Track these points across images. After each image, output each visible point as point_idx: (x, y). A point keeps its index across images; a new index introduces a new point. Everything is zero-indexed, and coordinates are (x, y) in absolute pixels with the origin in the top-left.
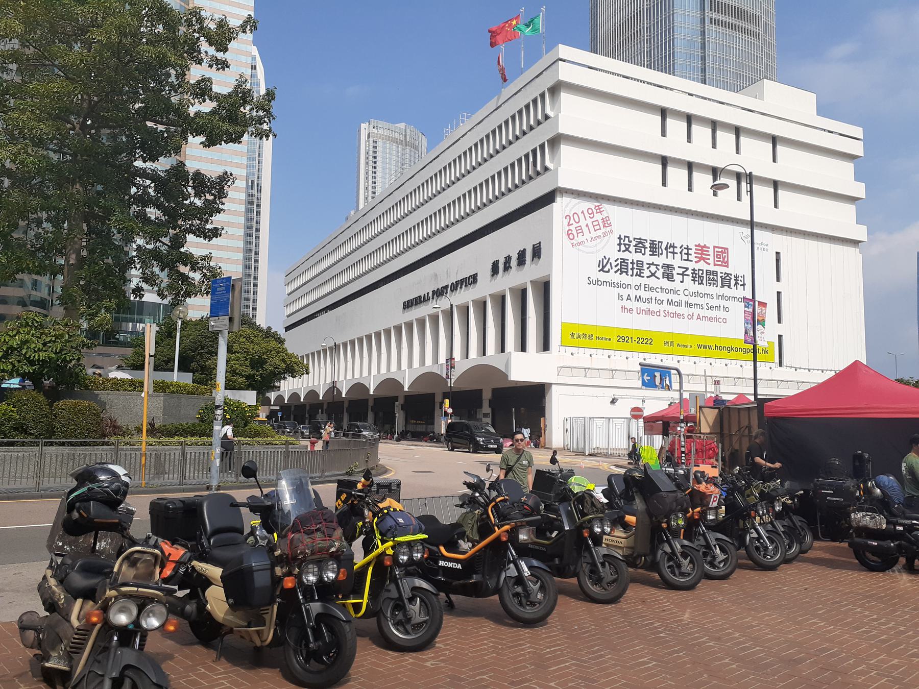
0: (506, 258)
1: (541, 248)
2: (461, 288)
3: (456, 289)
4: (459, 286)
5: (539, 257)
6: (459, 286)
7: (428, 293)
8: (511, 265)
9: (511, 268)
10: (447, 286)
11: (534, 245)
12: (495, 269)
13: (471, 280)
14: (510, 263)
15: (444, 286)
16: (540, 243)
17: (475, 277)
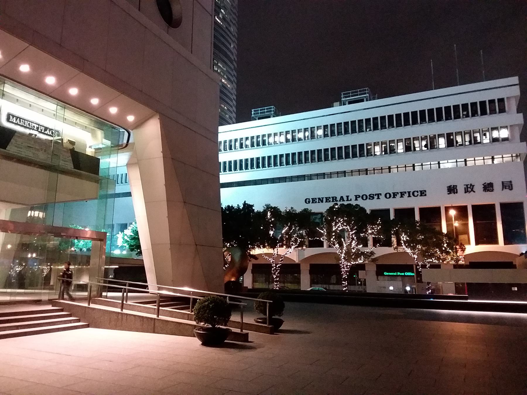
0: (467, 185)
1: (512, 185)
4: (400, 195)
5: (511, 189)
7: (348, 197)
9: (474, 192)
10: (381, 194)
11: (503, 182)
13: (416, 194)
16: (511, 182)
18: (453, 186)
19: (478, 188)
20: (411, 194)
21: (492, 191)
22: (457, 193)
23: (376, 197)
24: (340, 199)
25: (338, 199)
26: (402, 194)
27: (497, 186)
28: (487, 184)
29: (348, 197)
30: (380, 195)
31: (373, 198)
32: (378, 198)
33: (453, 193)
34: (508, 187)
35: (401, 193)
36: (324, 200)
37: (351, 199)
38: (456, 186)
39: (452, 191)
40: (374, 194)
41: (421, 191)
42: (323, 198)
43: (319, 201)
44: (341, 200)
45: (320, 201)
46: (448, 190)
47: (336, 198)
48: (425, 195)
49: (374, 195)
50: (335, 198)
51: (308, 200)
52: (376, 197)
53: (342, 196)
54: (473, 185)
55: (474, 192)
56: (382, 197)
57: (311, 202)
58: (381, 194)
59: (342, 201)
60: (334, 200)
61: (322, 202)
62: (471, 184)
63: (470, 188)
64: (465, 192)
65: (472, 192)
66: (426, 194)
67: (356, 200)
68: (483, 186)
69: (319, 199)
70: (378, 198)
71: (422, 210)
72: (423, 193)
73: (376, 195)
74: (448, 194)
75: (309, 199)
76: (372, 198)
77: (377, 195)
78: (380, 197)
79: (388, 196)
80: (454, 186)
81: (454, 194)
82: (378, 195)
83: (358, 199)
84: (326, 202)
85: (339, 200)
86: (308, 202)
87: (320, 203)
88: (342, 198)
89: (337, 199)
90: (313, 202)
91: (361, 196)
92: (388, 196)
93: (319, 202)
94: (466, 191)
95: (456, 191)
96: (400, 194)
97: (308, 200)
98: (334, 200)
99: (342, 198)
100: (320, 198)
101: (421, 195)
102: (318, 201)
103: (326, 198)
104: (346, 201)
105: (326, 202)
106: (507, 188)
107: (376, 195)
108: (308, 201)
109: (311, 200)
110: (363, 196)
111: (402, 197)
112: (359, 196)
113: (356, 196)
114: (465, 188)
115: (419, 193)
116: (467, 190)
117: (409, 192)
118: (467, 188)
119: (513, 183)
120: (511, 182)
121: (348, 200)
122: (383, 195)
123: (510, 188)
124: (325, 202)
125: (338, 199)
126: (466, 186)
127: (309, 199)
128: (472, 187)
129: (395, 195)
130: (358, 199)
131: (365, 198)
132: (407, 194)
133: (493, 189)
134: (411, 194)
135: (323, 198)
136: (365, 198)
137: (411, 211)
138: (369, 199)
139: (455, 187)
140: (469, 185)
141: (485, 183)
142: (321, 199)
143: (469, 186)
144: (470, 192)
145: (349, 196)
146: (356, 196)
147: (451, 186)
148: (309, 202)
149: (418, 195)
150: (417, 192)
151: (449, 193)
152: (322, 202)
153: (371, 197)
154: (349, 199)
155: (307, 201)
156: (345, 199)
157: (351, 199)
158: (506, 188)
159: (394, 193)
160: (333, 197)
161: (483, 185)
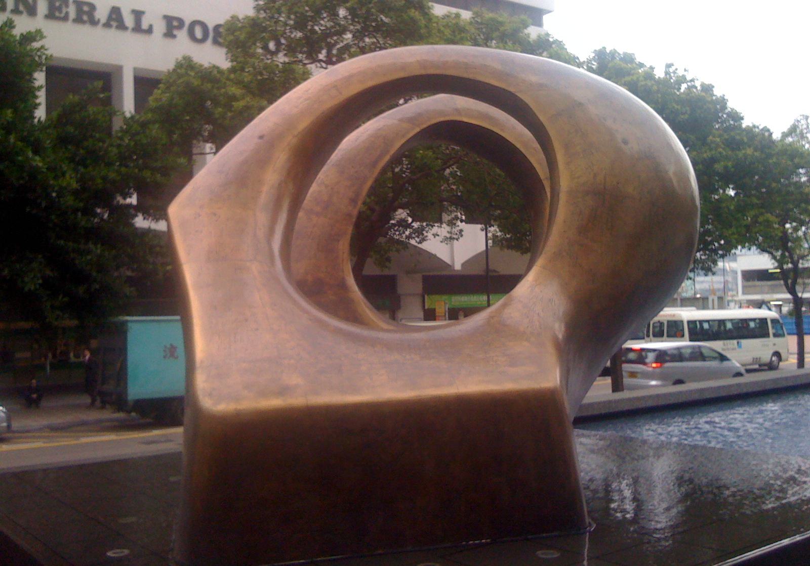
24: (110, 18)
25: (102, 14)
37: (151, 27)
45: (21, 8)
47: (92, 7)
59: (118, 27)
60: (85, 18)
83: (175, 32)
85: (103, 20)
88: (115, 17)
91: (187, 23)
98: (85, 18)
99: (115, 17)
110: (194, 23)
112: (181, 22)
121: (138, 29)
130: (175, 32)
131: (199, 33)
136: (199, 33)
146: (169, 19)
154: (145, 26)
156: (129, 21)
157: (151, 27)
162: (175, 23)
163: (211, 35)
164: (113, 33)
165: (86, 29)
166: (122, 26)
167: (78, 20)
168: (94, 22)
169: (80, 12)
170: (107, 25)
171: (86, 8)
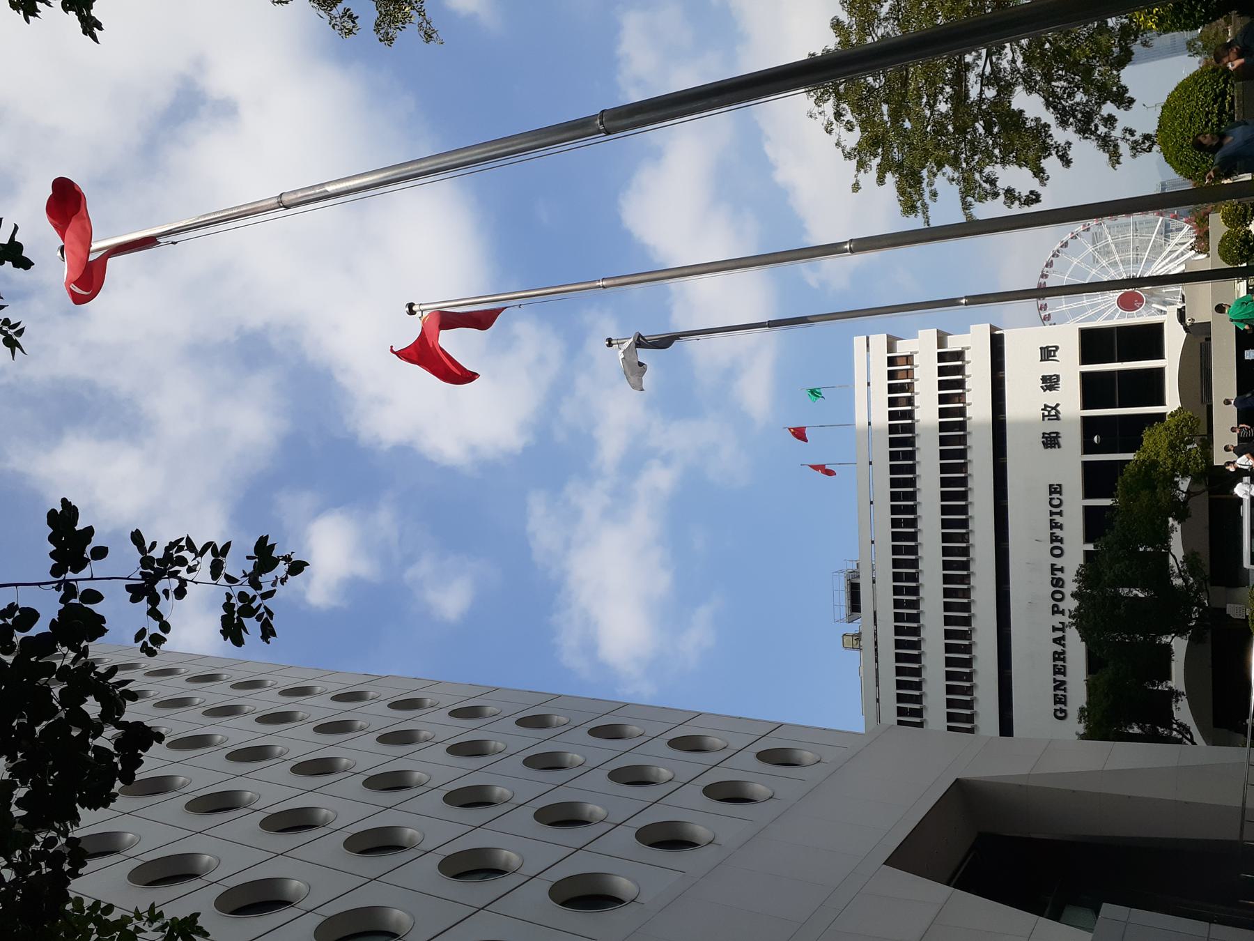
0: (1044, 416)
1: (1048, 347)
2: (1061, 527)
3: (1061, 541)
4: (1057, 532)
5: (1057, 348)
6: (1057, 532)
8: (1054, 406)
9: (1058, 405)
10: (1053, 565)
12: (1051, 441)
13: (1056, 502)
14: (1053, 408)
15: (1049, 577)
16: (1041, 348)
17: (1055, 490)
18: (1044, 440)
19: (1051, 398)
20: (1056, 509)
21: (1058, 377)
22: (1057, 433)
23: (1059, 574)
24: (1060, 644)
25: (1059, 648)
26: (1054, 525)
27: (1049, 368)
28: (1044, 385)
29: (1054, 629)
30: (1055, 567)
31: (1060, 579)
32: (1061, 570)
33: (1059, 439)
34: (1053, 353)
35: (1052, 528)
36: (1060, 677)
38: (1044, 434)
39: (1054, 441)
40: (1052, 578)
41: (1051, 493)
42: (1055, 681)
43: (1061, 690)
44: (1062, 642)
46: (1051, 447)
47: (1055, 653)
48: (1060, 485)
49: (1055, 578)
50: (1057, 656)
51: (1059, 714)
52: (1059, 574)
53: (1053, 639)
54: (1043, 407)
55: (1058, 405)
56: (1059, 562)
57: (1062, 706)
58: (1053, 565)
60: (1062, 657)
61: (1063, 683)
62: (1042, 410)
63: (1049, 412)
64: (1058, 419)
65: (1058, 408)
66: (1057, 485)
67: (1063, 612)
68: (1048, 391)
69: (1056, 688)
70: (1061, 570)
71: (1088, 494)
72: (1055, 490)
73: (1052, 574)
74: (1059, 447)
75: (1056, 710)
76: (1061, 583)
77: (1056, 572)
78: (1059, 566)
79: (1057, 552)
80: (1043, 438)
81: (1059, 437)
82: (1054, 569)
83: (1061, 610)
84: (1064, 674)
85: (1062, 648)
86: (1063, 714)
87: (1065, 688)
89: (1060, 651)
90: (1065, 703)
92: (1057, 552)
93: (1065, 690)
94: (1055, 417)
95: (1055, 435)
96: (1054, 530)
97: (1059, 714)
98: (1062, 657)
100: (1054, 687)
101: (1060, 493)
102: (1062, 693)
103: (1055, 673)
104: (1063, 632)
105: (1064, 674)
106: (1054, 353)
107: (1056, 575)
108: (1061, 713)
109: (1058, 706)
111: (1061, 527)
112: (1054, 606)
113: (1054, 613)
114: (1049, 419)
115: (1054, 496)
116: (1053, 416)
117: (1052, 513)
118: (1049, 415)
119: (1045, 346)
120: (1041, 348)
122: (1055, 560)
123: (1054, 349)
124: (1065, 676)
125: (1059, 648)
126: (1046, 418)
127: (1056, 710)
128: (1049, 409)
129: (1054, 538)
131: (1058, 596)
132: (1054, 517)
133: (1054, 375)
134: (1056, 509)
135: (1054, 679)
136: (1058, 596)
137: (1090, 514)
138: (1062, 586)
139: (1047, 435)
140: (1043, 414)
141: (1042, 387)
142: (1058, 683)
143: (1046, 413)
144: (1058, 412)
145: (1053, 626)
146: (1054, 613)
147: (1043, 442)
148: (1062, 711)
149: (1058, 498)
150: (1051, 499)
151: (1057, 446)
152: (1063, 683)
153: (1058, 583)
154: (1061, 626)
155: (1061, 715)
156: (1059, 634)
158: (1054, 356)
159: (1052, 541)
160: (1055, 659)
161: (1045, 391)
162: (1056, 609)
163: (1058, 589)
164: (1067, 642)
165: (1068, 656)
166: (1063, 638)
167: (1064, 660)
168: (1063, 653)
169: (1059, 659)
170: (1064, 645)
171: (1057, 656)
